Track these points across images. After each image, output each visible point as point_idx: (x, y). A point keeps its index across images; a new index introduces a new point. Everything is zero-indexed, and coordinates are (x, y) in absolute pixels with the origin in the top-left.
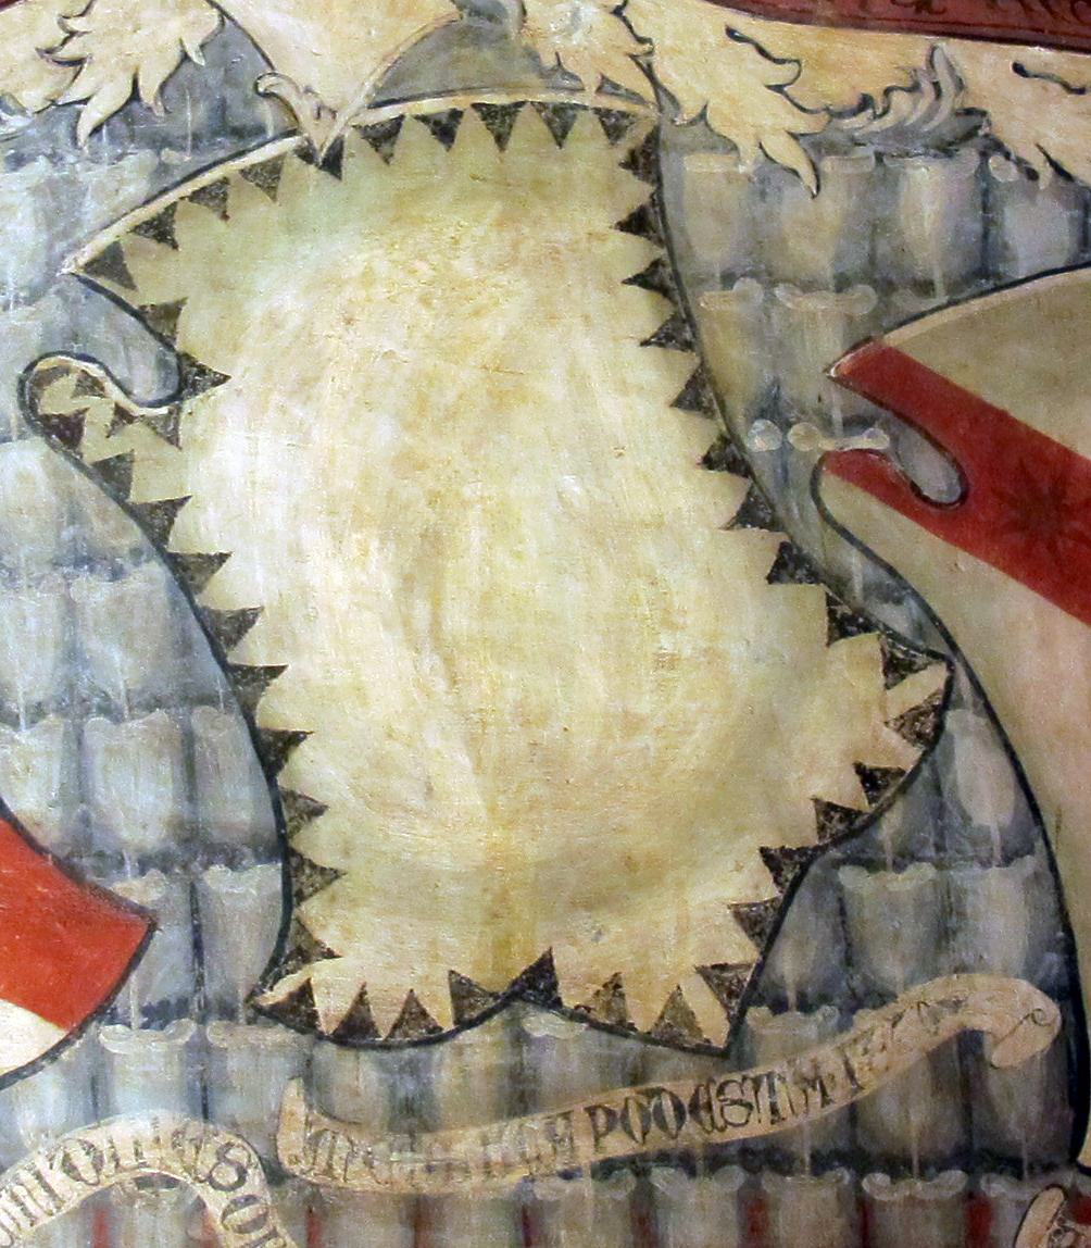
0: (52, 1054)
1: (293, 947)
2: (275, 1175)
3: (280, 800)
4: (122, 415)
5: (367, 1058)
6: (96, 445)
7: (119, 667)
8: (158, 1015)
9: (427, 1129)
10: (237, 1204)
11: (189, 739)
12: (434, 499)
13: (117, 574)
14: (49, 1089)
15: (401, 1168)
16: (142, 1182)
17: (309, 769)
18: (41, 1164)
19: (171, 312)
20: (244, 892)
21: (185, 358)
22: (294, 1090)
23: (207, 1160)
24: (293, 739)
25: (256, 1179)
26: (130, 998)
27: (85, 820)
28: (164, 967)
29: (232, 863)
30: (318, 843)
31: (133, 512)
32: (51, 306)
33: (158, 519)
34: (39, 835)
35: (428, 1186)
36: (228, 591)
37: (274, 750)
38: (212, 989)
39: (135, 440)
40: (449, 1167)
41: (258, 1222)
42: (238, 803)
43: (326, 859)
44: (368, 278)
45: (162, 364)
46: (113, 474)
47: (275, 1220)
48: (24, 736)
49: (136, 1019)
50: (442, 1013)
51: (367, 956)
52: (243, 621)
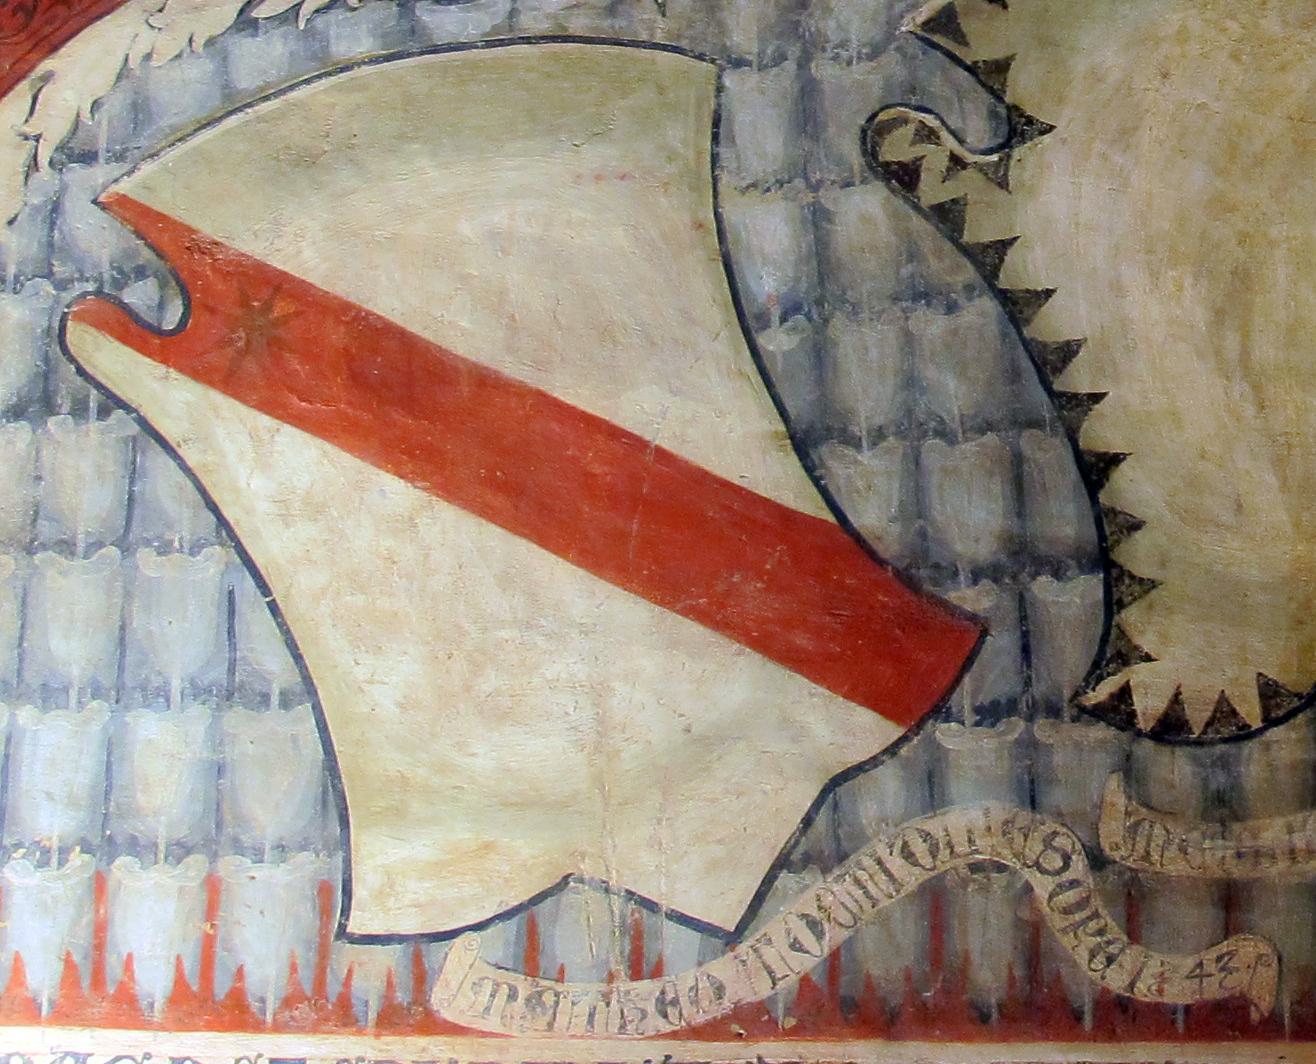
0: (892, 750)
1: (1114, 651)
2: (1098, 861)
3: (1102, 516)
4: (957, 162)
5: (1181, 753)
6: (932, 190)
7: (954, 393)
8: (990, 714)
9: (1237, 818)
10: (1062, 888)
11: (1018, 460)
12: (1243, 239)
13: (951, 308)
14: (889, 782)
15: (1213, 855)
16: (975, 867)
17: (1129, 488)
18: (882, 851)
19: (1001, 67)
20: (1068, 601)
21: (1014, 109)
22: (1114, 783)
23: (1035, 848)
24: (1115, 460)
25: (1079, 864)
26: (964, 698)
27: (923, 534)
28: (995, 670)
29: (1058, 574)
30: (1137, 555)
31: (966, 251)
32: (891, 60)
33: (990, 258)
34: (880, 549)
35: (1238, 871)
36: (1054, 324)
37: (1096, 469)
38: (1039, 690)
39: (968, 184)
40: (1257, 853)
41: (1081, 904)
42: (1063, 519)
43: (1144, 570)
44: (1182, 36)
45: (993, 115)
46: (948, 216)
47: (1097, 902)
48: (866, 457)
49: (970, 717)
50: (1251, 712)
51: (1182, 660)
52: (1068, 351)
